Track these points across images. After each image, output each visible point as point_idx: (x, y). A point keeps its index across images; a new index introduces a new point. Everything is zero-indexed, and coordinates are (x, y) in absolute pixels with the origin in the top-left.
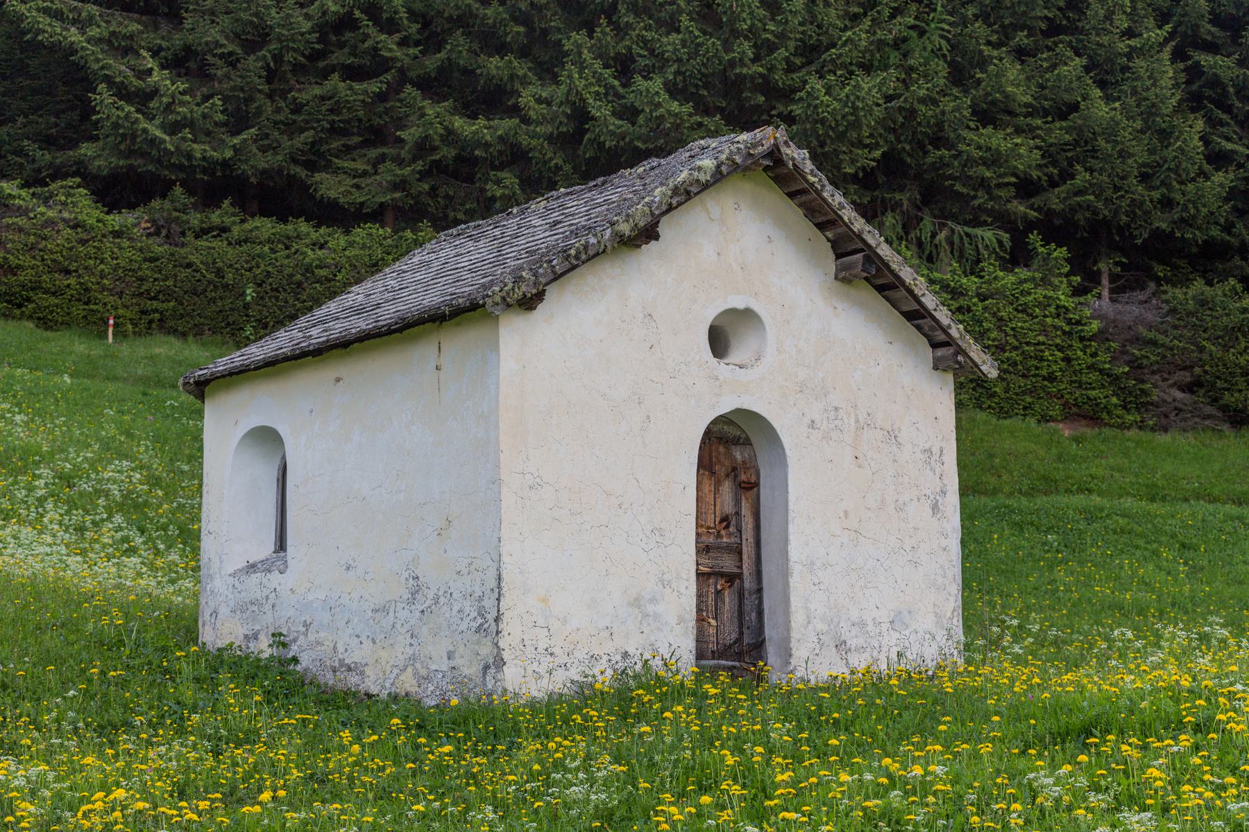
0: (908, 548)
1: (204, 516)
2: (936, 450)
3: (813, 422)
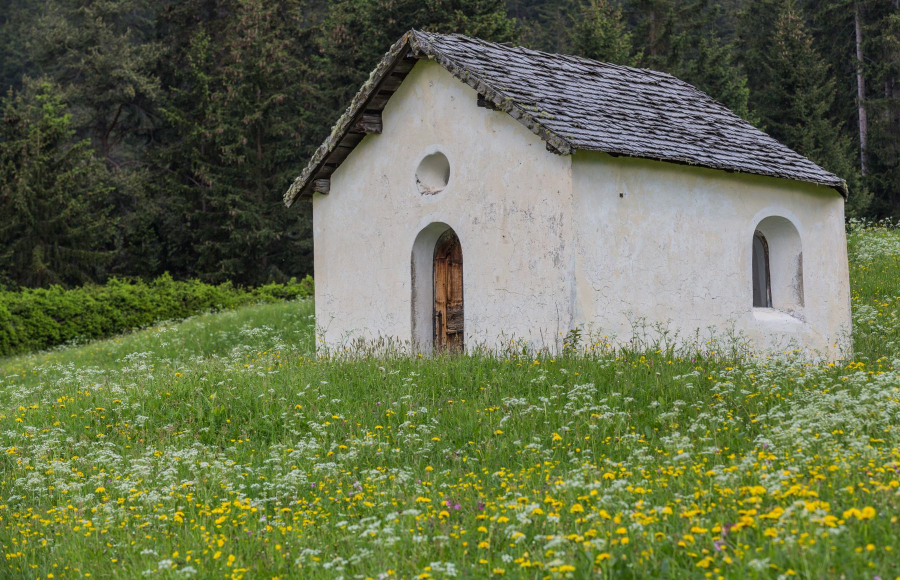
0: (536, 294)
1: (847, 262)
2: (558, 217)
3: (476, 219)
